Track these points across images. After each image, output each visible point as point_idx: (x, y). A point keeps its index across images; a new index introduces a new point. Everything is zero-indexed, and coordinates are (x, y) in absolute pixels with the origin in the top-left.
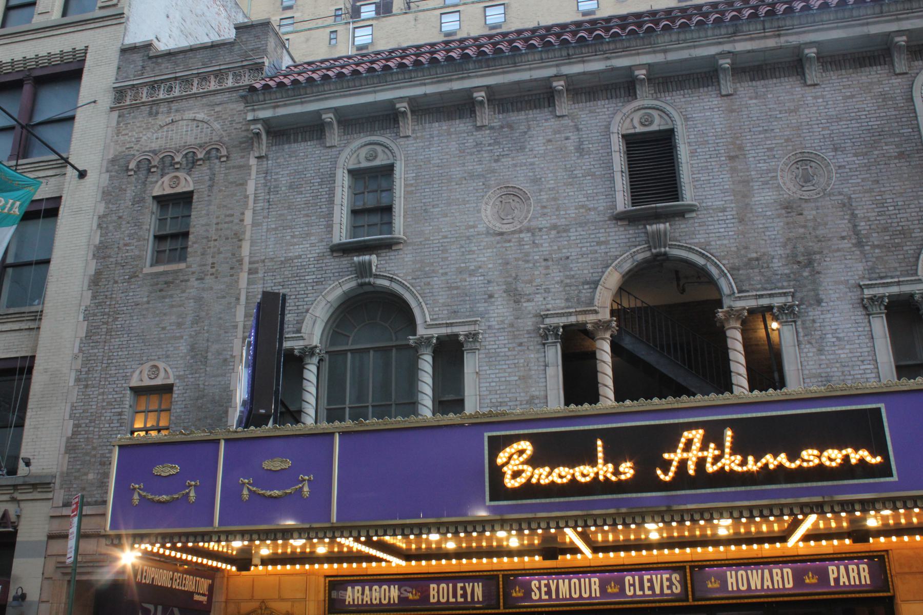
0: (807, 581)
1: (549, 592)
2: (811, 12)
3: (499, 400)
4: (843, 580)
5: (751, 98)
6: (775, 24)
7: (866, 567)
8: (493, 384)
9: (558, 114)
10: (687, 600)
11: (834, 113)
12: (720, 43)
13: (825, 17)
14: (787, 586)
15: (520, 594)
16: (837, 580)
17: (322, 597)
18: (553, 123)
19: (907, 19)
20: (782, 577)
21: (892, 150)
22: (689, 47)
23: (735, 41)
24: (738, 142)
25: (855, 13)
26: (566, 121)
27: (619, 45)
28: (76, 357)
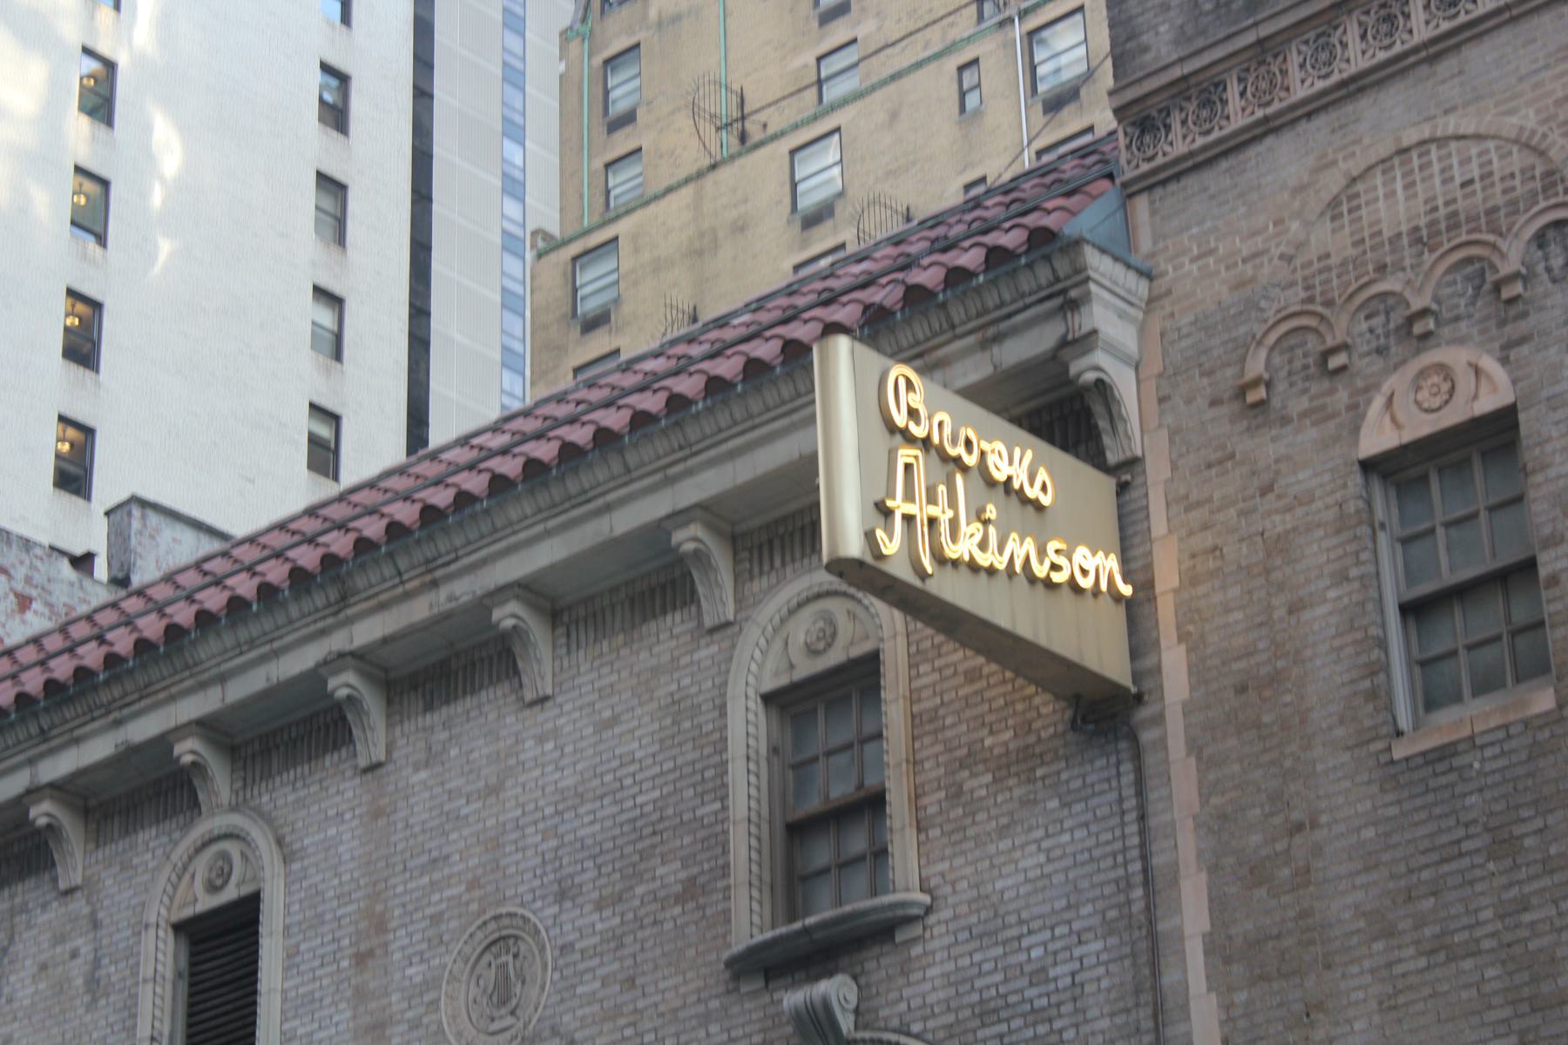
2: (478, 507)
5: (417, 769)
6: (418, 556)
9: (62, 885)
11: (570, 782)
12: (323, 633)
13: (513, 512)
18: (55, 913)
19: (690, 472)
21: (671, 874)
22: (263, 659)
23: (350, 621)
24: (379, 908)
25: (572, 486)
26: (79, 905)
27: (129, 686)
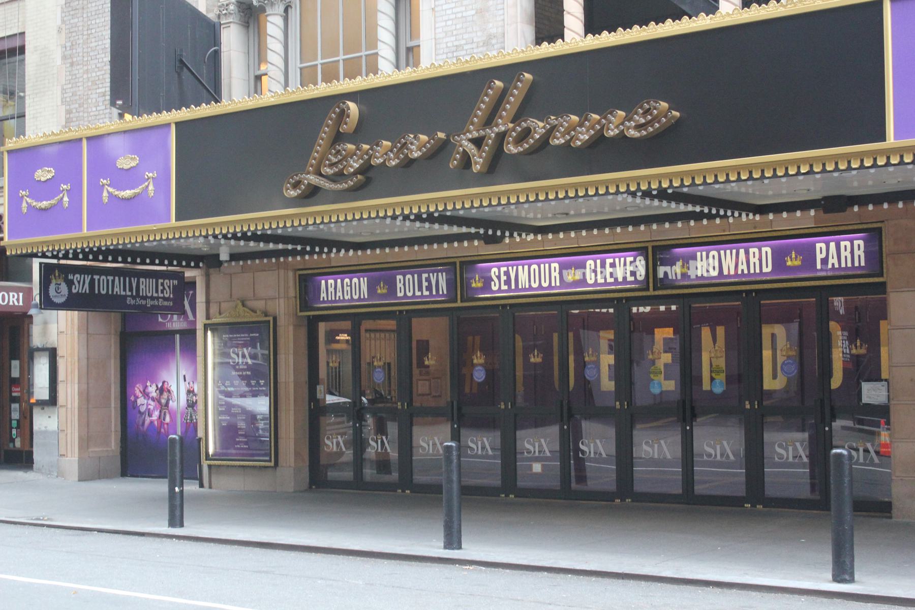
0: (789, 263)
1: (508, 282)
3: (456, 43)
4: (833, 261)
7: (861, 242)
8: (449, 23)
10: (647, 289)
14: (765, 270)
15: (480, 285)
16: (825, 261)
17: (292, 293)
20: (760, 260)
28: (59, 31)
